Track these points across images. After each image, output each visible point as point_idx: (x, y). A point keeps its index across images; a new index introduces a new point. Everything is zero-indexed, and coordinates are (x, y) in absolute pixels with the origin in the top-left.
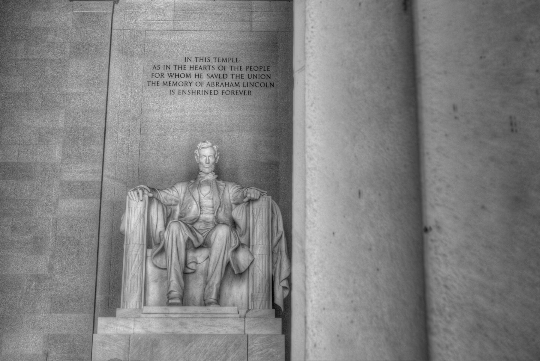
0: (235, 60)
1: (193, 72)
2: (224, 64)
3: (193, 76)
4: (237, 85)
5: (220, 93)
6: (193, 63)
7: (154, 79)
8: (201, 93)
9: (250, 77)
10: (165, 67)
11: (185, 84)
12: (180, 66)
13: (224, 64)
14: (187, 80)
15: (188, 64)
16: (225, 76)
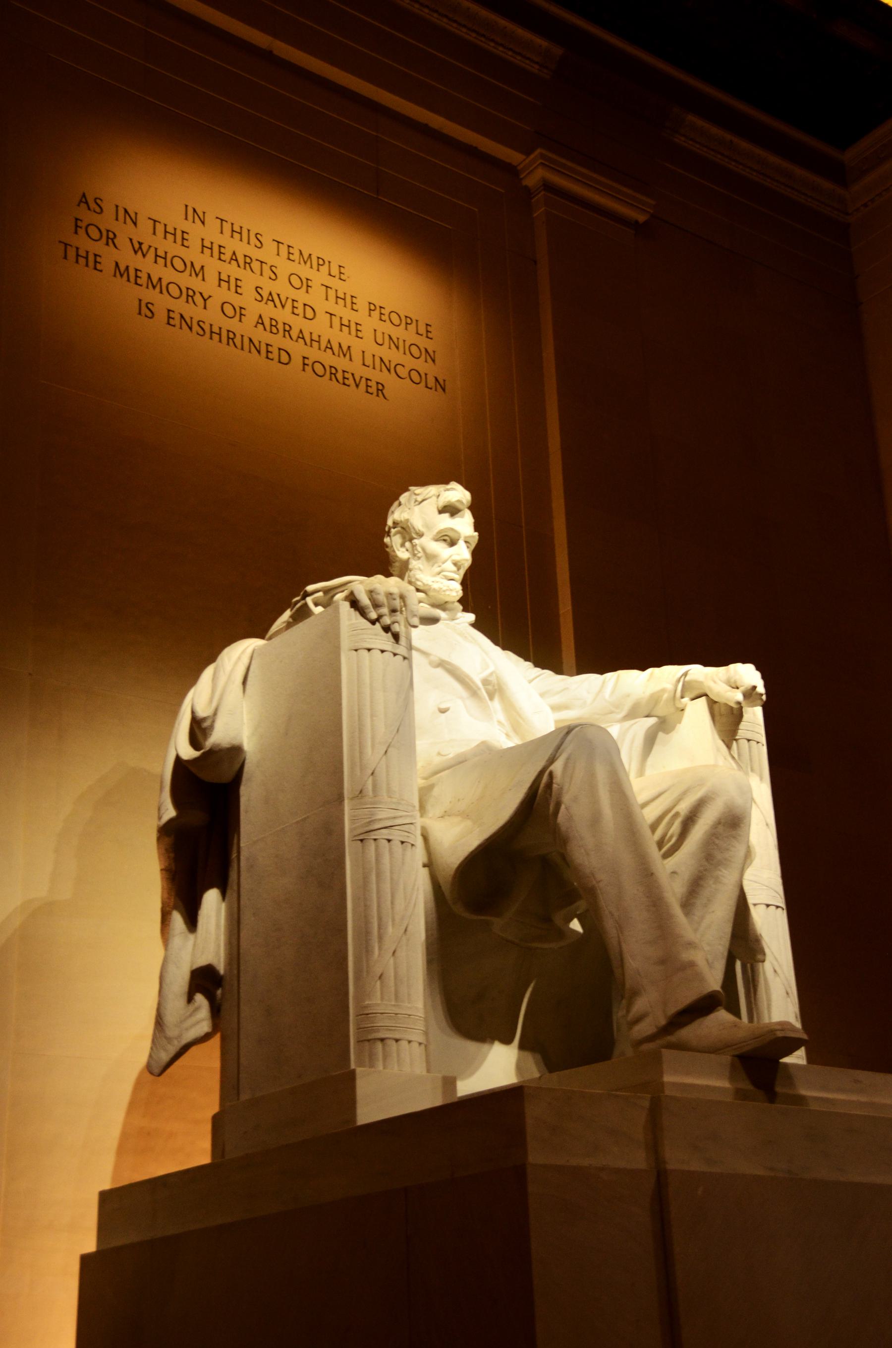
0: (335, 271)
1: (213, 266)
2: (305, 271)
3: (211, 275)
4: (346, 352)
5: (297, 361)
6: (211, 233)
7: (83, 242)
8: (238, 341)
9: (380, 341)
10: (121, 213)
11: (190, 294)
12: (170, 229)
13: (305, 271)
14: (195, 283)
15: (196, 232)
16: (310, 314)
